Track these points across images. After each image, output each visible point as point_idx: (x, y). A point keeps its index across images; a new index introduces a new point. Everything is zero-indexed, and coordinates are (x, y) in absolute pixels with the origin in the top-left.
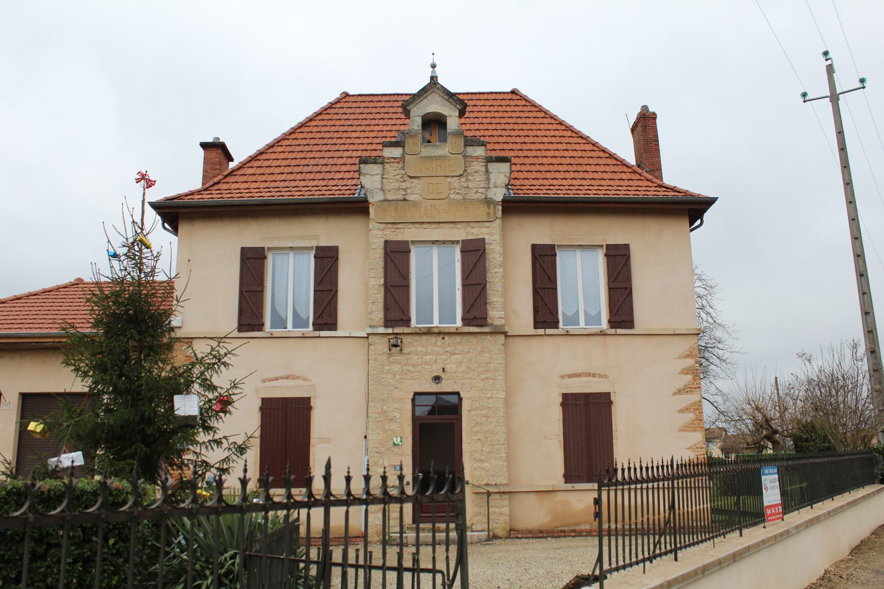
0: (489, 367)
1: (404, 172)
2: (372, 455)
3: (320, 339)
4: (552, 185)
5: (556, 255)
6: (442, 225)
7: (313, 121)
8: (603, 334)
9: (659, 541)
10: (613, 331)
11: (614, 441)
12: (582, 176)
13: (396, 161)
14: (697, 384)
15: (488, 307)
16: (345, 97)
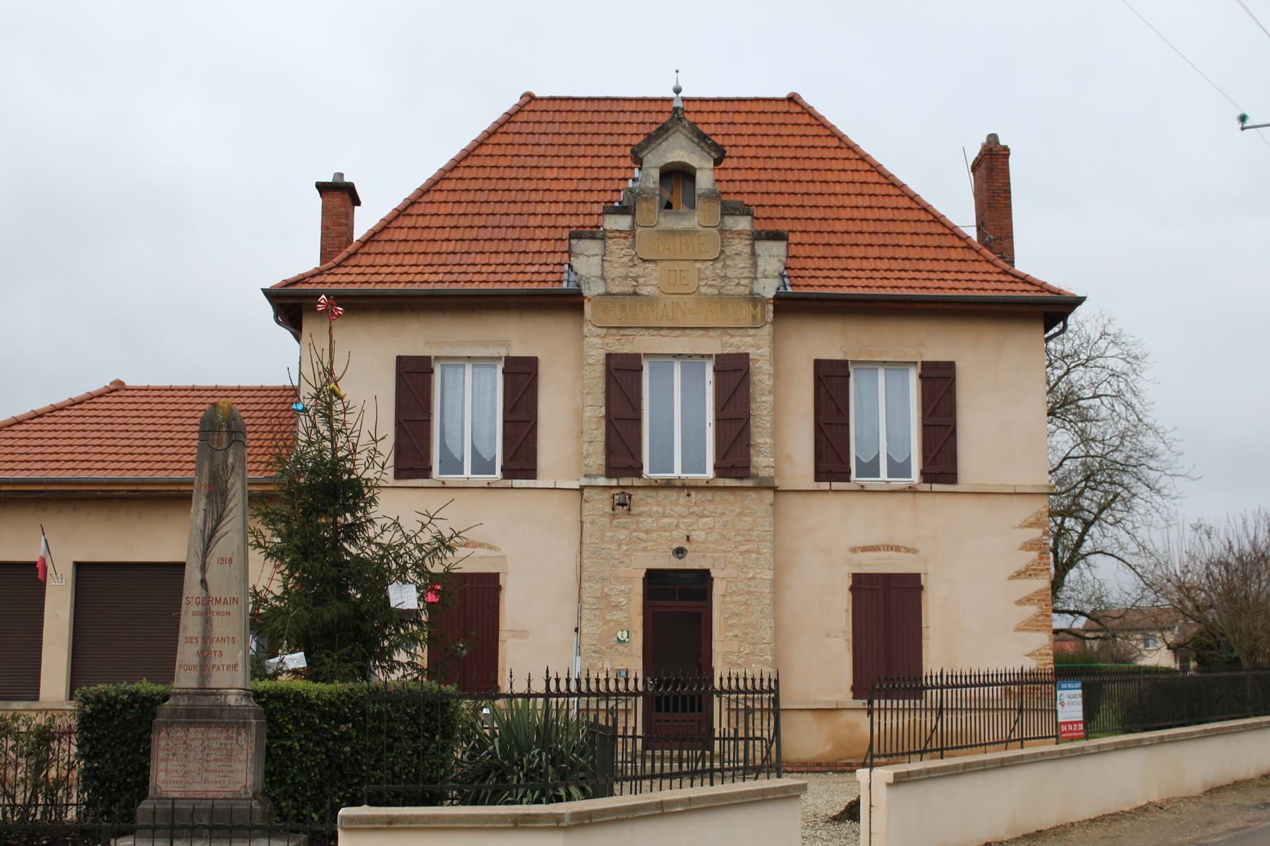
0: (751, 536)
1: (633, 253)
2: (588, 655)
3: (512, 490)
4: (847, 269)
5: (848, 376)
6: (687, 332)
8: (912, 490)
9: (926, 742)
10: (926, 487)
11: (924, 642)
14: (1045, 564)
15: (752, 452)
16: (530, 102)
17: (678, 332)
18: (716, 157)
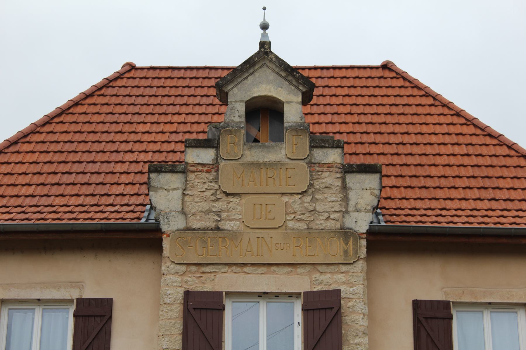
1: (217, 187)
5: (451, 318)
6: (273, 268)
7: (80, 106)
12: (492, 196)
13: (206, 169)
16: (129, 71)
17: (264, 269)
18: (304, 90)
